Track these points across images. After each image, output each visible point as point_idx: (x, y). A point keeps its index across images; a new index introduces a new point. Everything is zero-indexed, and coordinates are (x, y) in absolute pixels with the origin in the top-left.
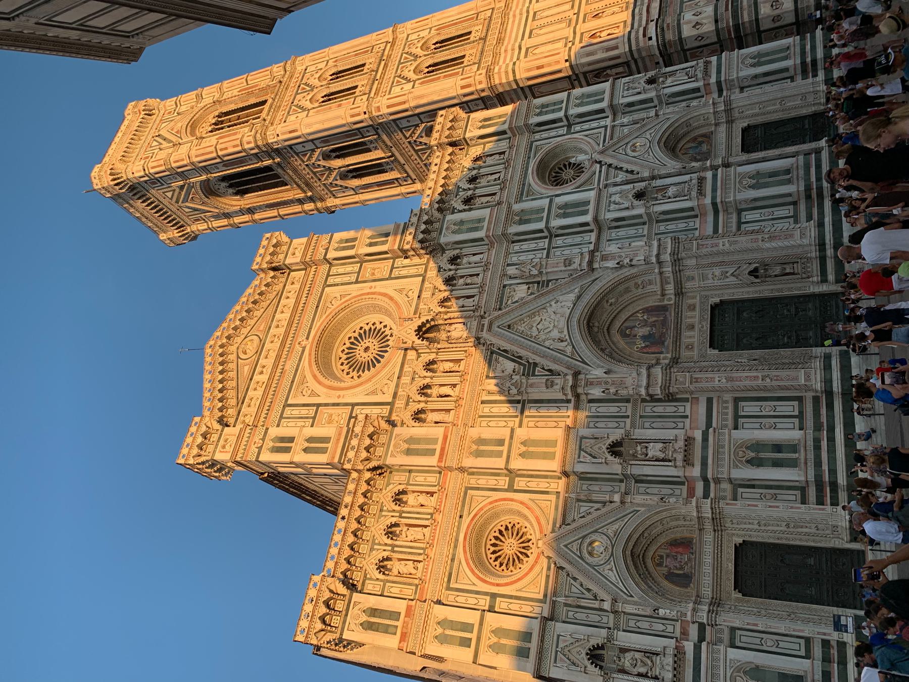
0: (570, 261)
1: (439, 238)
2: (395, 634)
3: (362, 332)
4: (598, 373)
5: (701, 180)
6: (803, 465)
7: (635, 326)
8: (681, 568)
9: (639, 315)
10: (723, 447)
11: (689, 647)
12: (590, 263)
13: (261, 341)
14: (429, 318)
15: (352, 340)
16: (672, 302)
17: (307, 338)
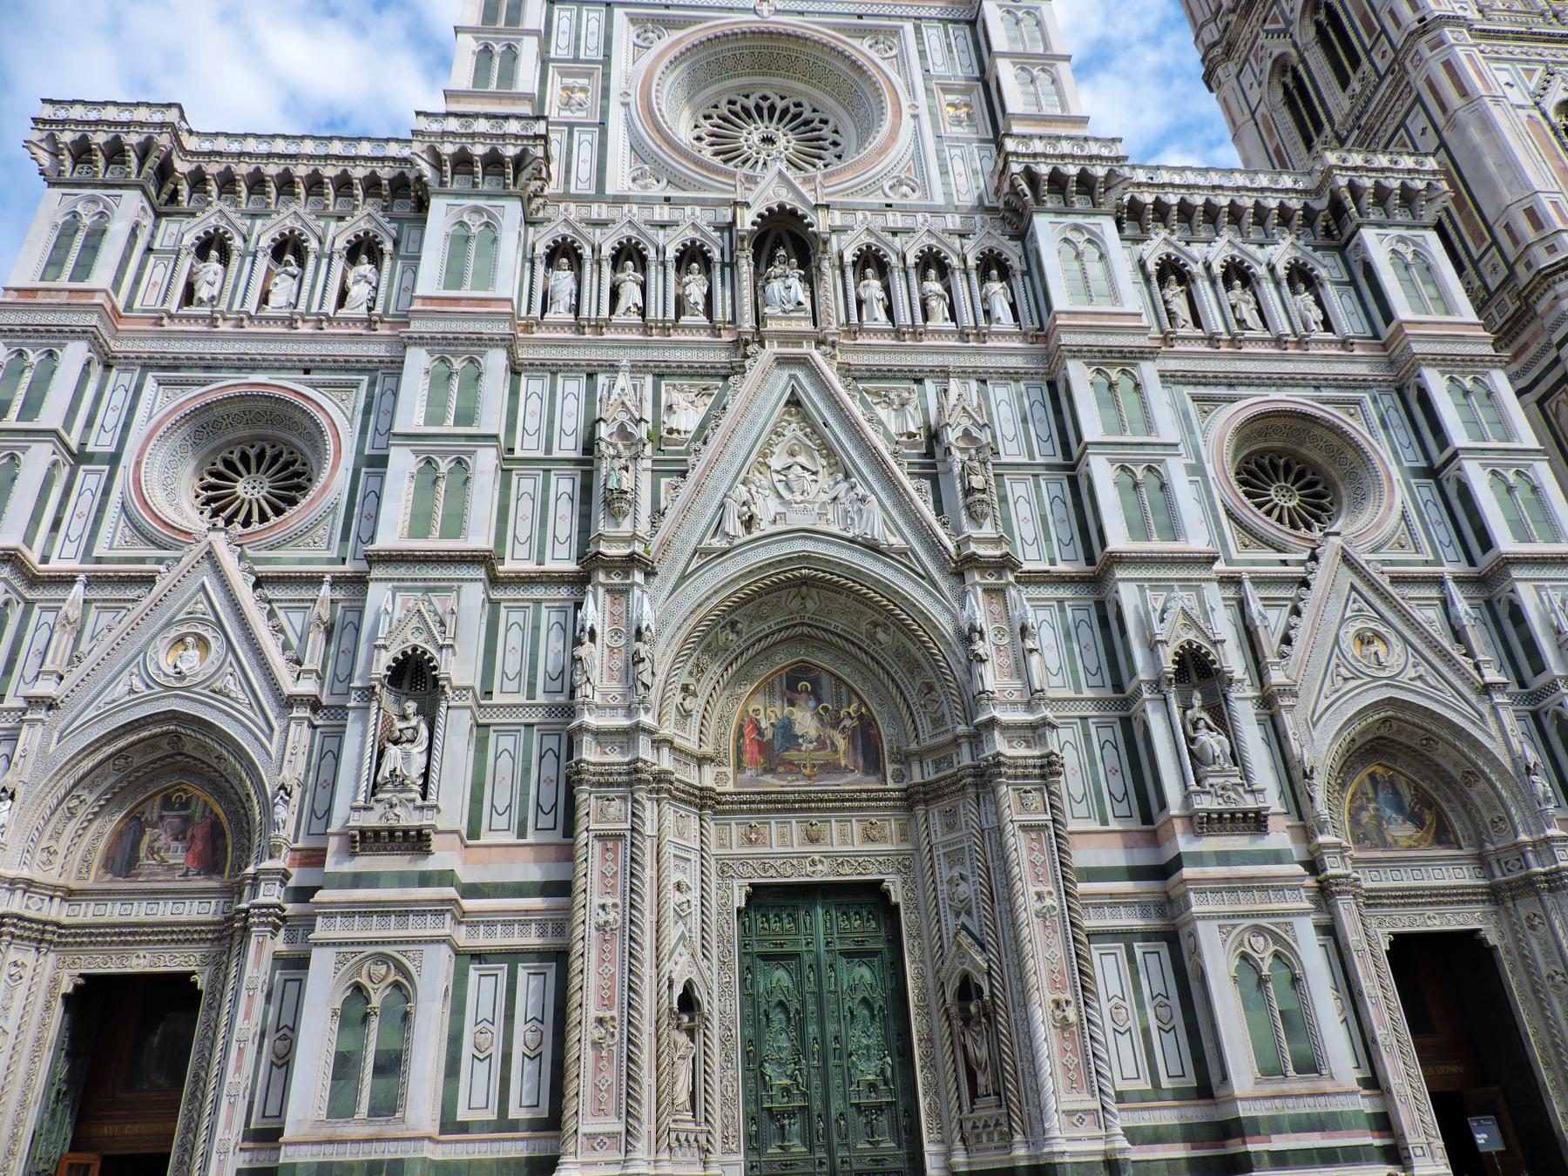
0: (986, 515)
2: (42, 279)
3: (816, 124)
5: (1256, 822)
6: (325, 1132)
7: (819, 701)
8: (152, 851)
9: (854, 706)
12: (972, 561)
15: (793, 110)
17: (778, 12)
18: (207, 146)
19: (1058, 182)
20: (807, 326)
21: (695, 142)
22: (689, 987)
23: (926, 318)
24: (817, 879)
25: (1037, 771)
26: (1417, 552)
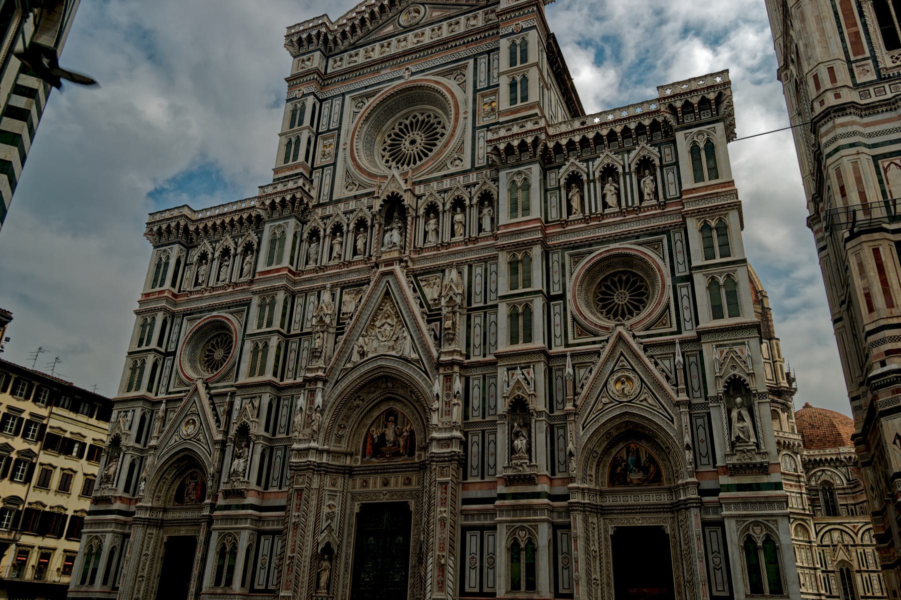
0: (452, 340)
1: (504, 168)
2: (152, 288)
3: (435, 125)
4: (319, 400)
5: (530, 480)
6: (212, 591)
7: (396, 425)
9: (408, 427)
10: (236, 524)
11: (117, 506)
13: (418, 24)
14: (405, 203)
15: (426, 120)
16: (416, 460)
17: (413, 74)
18: (200, 216)
19: (509, 149)
20: (396, 255)
21: (383, 152)
22: (328, 544)
23: (453, 235)
24: (384, 501)
25: (447, 459)
26: (671, 327)
